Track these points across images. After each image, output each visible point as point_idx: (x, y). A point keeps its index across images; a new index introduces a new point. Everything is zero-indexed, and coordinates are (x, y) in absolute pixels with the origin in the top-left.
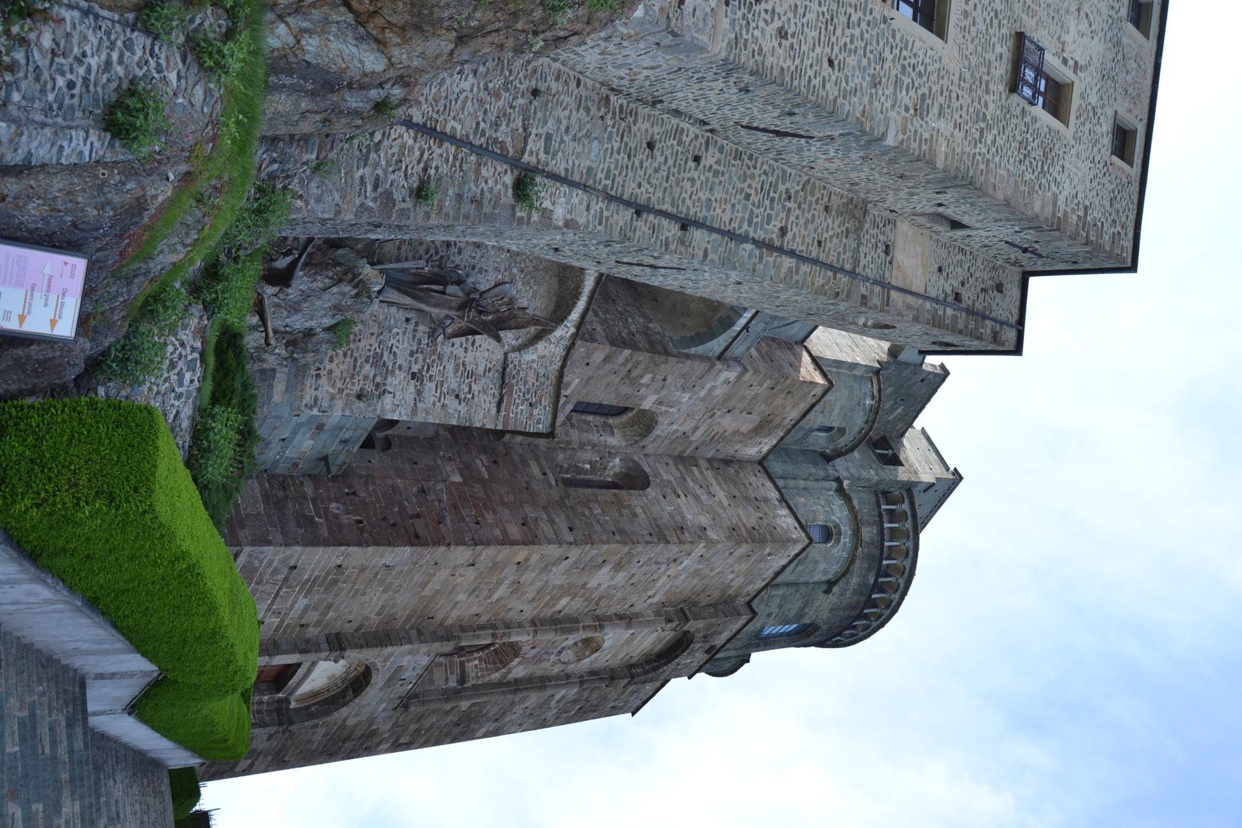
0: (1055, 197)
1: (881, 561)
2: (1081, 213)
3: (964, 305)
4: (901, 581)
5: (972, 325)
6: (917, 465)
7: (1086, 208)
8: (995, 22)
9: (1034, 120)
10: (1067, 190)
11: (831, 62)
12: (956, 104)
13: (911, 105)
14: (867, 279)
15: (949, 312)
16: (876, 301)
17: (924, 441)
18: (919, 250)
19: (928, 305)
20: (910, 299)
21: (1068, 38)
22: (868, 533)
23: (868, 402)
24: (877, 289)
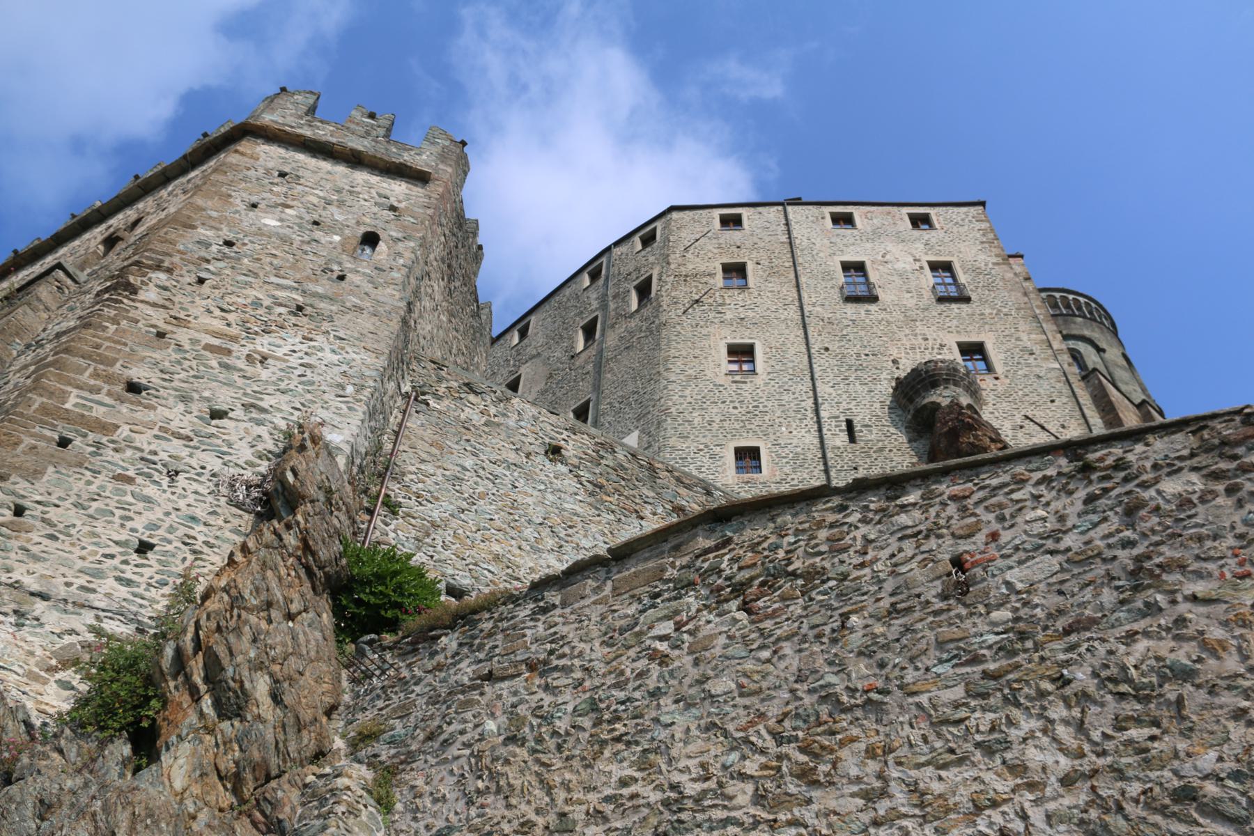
0: (994, 264)
4: (1071, 297)
11: (1052, 401)
12: (1007, 332)
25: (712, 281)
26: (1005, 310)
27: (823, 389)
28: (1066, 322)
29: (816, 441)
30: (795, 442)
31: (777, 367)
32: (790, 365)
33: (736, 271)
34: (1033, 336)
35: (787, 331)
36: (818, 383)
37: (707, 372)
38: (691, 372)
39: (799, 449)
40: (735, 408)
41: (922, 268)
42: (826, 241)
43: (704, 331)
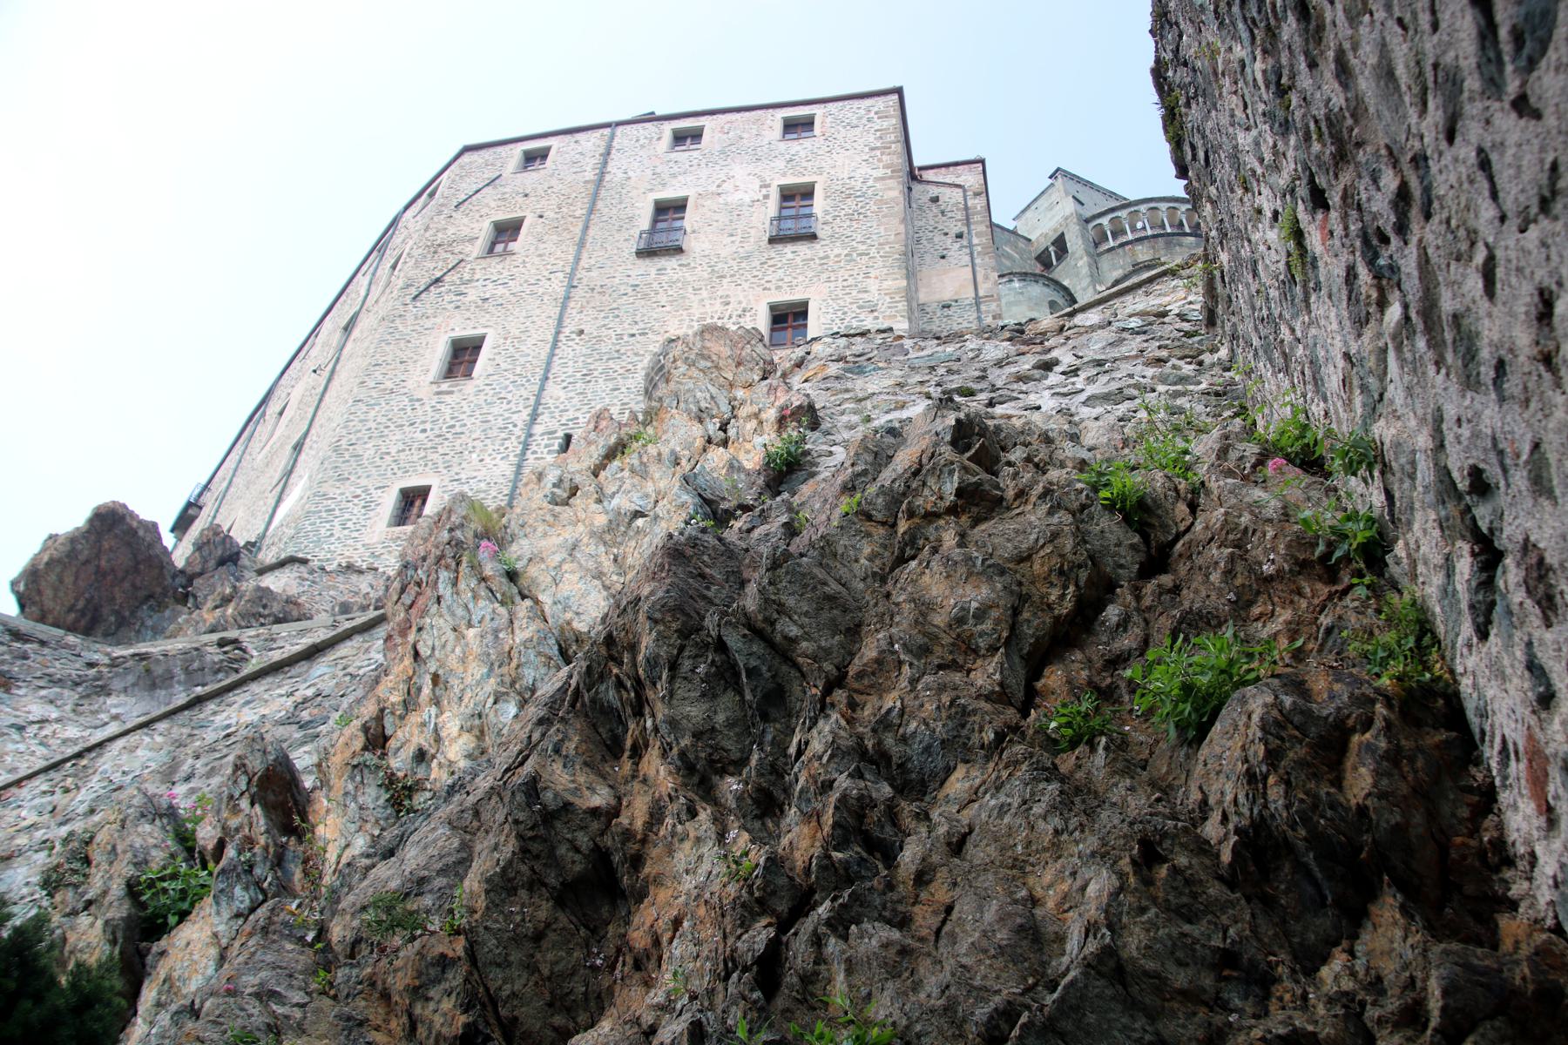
0: (877, 179)
1: (1169, 235)
2: (878, 153)
3: (965, 229)
5: (977, 218)
6: (1058, 218)
7: (872, 149)
8: (771, 263)
9: (827, 213)
10: (865, 170)
12: (851, 281)
13: (872, 316)
14: (979, 318)
15: (975, 241)
16: (993, 306)
17: (1028, 214)
18: (934, 280)
19: (978, 261)
20: (980, 278)
21: (747, 199)
22: (1143, 253)
23: (1016, 284)
24: (983, 308)
25: (468, 248)
26: (862, 248)
27: (553, 389)
28: (1168, 245)
29: (510, 471)
30: (480, 475)
31: (503, 366)
32: (522, 360)
33: (507, 231)
34: (886, 284)
35: (538, 312)
36: (550, 383)
37: (410, 384)
38: (389, 385)
39: (483, 486)
40: (424, 431)
41: (766, 197)
42: (649, 172)
43: (428, 324)
